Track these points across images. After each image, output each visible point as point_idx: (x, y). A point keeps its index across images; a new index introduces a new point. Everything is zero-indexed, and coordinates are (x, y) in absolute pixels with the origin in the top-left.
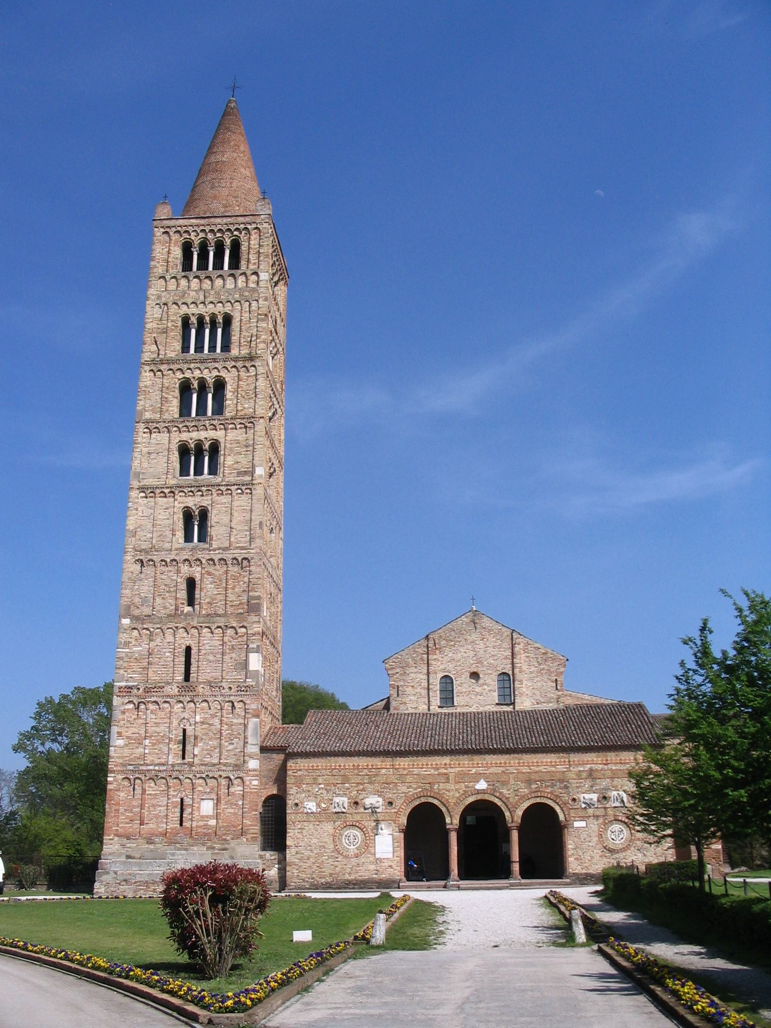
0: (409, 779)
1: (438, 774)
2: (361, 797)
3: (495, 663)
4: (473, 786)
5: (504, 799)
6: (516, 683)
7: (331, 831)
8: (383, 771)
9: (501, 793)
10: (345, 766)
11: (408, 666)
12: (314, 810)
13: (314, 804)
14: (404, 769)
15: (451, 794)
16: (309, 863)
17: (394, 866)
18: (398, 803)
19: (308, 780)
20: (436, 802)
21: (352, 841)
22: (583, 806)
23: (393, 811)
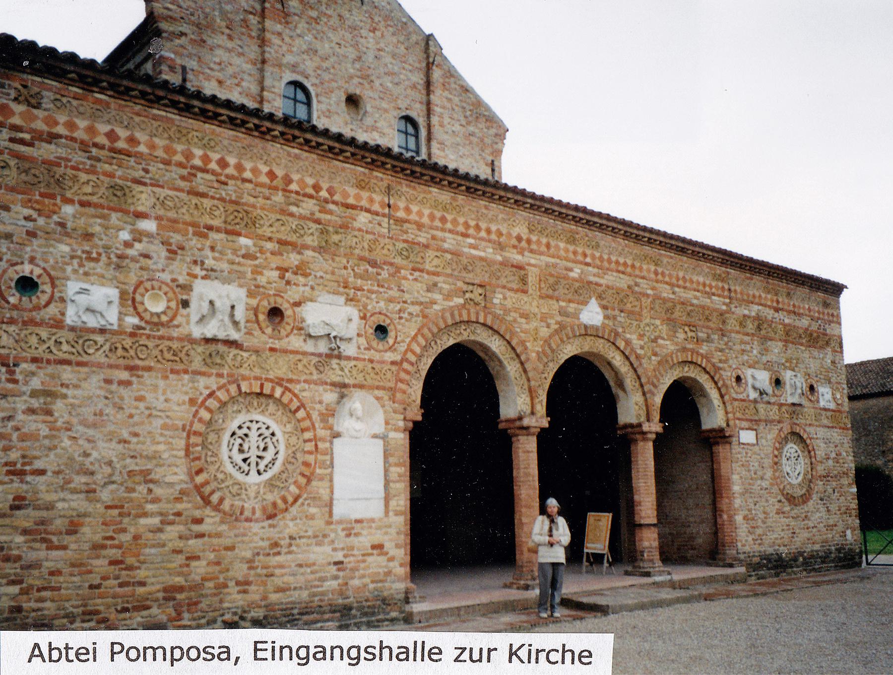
0: (431, 261)
1: (504, 264)
2: (293, 294)
3: (396, 91)
4: (576, 315)
5: (633, 358)
6: (434, 144)
7: (181, 413)
8: (363, 219)
9: (628, 342)
10: (240, 168)
11: (210, 26)
12: (112, 317)
13: (113, 293)
14: (420, 226)
15: (534, 324)
16: (76, 547)
17: (389, 546)
18: (405, 331)
19: (85, 185)
20: (495, 345)
21: (253, 454)
22: (753, 395)
23: (389, 356)
